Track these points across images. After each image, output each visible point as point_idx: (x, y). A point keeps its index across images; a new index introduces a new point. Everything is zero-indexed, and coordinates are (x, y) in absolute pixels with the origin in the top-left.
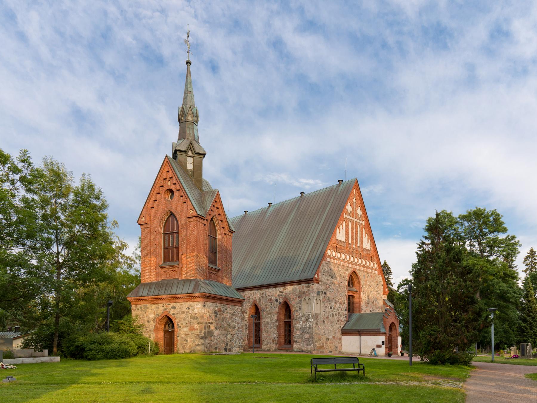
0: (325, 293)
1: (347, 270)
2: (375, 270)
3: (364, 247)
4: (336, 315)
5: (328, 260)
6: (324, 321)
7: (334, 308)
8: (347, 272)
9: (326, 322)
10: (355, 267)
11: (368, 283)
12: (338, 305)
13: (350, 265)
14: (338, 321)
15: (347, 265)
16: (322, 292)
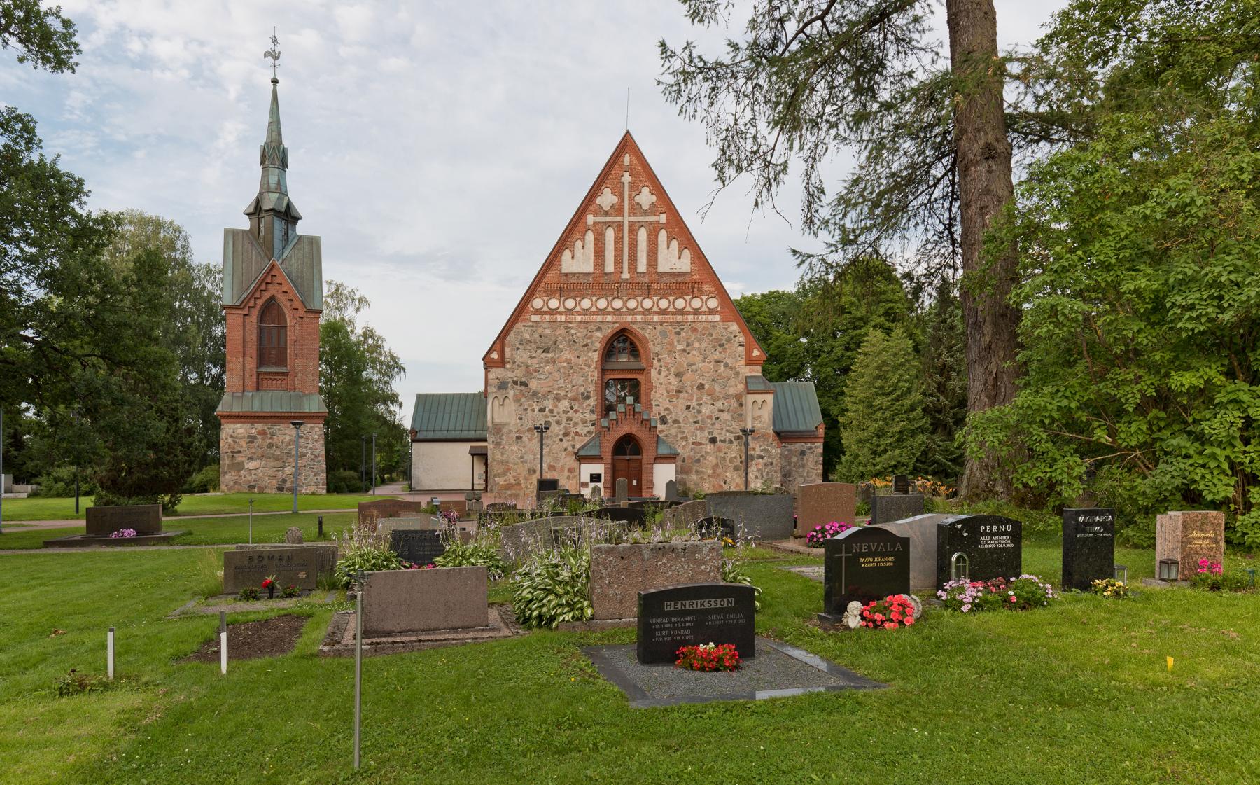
0: (524, 384)
1: (599, 329)
3: (661, 269)
4: (558, 423)
5: (535, 318)
6: (519, 438)
8: (598, 334)
9: (525, 439)
10: (630, 318)
11: (680, 347)
12: (564, 404)
13: (609, 318)
14: (566, 434)
15: (599, 318)
16: (516, 383)
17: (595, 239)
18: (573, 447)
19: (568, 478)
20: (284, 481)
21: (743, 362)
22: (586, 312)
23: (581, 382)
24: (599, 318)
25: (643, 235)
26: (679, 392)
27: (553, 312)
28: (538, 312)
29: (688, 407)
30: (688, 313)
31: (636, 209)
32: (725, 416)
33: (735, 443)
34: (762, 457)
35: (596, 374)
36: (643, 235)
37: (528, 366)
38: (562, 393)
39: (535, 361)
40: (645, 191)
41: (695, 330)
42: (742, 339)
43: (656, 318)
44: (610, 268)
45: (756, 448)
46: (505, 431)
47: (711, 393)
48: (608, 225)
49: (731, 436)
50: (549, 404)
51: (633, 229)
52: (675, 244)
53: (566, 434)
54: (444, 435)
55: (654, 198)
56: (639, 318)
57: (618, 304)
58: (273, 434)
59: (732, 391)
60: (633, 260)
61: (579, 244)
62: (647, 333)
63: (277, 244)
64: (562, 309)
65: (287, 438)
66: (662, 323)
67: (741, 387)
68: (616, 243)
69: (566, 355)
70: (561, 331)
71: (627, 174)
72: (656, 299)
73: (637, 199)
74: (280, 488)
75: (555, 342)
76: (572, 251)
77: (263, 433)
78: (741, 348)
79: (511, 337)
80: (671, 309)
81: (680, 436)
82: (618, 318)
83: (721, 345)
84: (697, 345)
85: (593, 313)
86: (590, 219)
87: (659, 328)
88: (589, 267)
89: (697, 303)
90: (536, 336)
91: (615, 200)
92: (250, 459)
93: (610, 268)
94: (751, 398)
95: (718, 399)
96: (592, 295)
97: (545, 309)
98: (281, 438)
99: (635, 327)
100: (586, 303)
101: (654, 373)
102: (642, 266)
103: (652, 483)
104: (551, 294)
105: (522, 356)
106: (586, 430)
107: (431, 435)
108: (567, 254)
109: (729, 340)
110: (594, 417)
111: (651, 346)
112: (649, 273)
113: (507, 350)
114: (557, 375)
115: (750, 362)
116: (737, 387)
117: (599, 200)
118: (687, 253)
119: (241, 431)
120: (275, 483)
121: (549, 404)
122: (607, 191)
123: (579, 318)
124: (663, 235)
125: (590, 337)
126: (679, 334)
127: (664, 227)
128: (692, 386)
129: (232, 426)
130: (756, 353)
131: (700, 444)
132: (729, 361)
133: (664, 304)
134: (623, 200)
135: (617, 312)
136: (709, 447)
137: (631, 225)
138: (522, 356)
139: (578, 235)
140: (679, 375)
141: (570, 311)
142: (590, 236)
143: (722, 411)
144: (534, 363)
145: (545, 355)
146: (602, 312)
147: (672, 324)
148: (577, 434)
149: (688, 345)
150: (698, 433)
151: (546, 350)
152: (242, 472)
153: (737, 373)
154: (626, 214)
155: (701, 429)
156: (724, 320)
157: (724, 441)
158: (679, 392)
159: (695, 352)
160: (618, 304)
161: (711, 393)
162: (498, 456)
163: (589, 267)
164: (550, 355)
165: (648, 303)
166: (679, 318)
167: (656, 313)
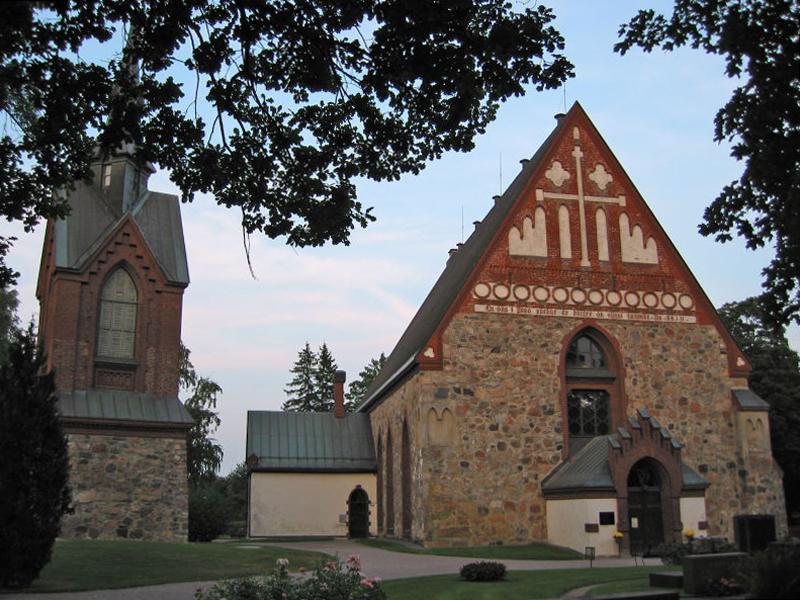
1: (559, 326)
2: (687, 312)
3: (626, 258)
6: (465, 465)
7: (506, 429)
8: (559, 332)
10: (594, 315)
11: (655, 352)
13: (571, 313)
15: (559, 313)
16: (458, 391)
18: (536, 477)
19: (531, 519)
20: (128, 521)
21: (726, 373)
22: (539, 304)
23: (541, 391)
25: (601, 218)
26: (659, 407)
27: (501, 302)
28: (482, 300)
30: (662, 312)
31: (590, 188)
32: (714, 438)
33: (728, 471)
34: (762, 490)
35: (559, 382)
36: (601, 218)
37: (473, 370)
38: (519, 406)
39: (481, 363)
40: (600, 169)
41: (670, 333)
42: (722, 345)
43: (625, 316)
44: (566, 252)
45: (756, 479)
46: (445, 454)
47: (695, 409)
48: (564, 203)
49: (723, 464)
50: (501, 418)
51: (591, 210)
52: (638, 230)
53: (526, 461)
54: (293, 464)
55: (610, 178)
56: (606, 315)
57: (579, 296)
58: (115, 451)
59: (719, 407)
61: (527, 222)
62: (616, 334)
63: (126, 198)
64: (512, 299)
65: (135, 458)
67: (728, 403)
70: (513, 325)
71: (577, 149)
74: (122, 532)
75: (507, 340)
76: (520, 229)
77: (102, 449)
78: (723, 356)
79: (449, 332)
80: (641, 306)
82: (582, 314)
83: (701, 352)
84: (674, 350)
87: (630, 328)
88: (541, 250)
89: (669, 301)
90: (482, 330)
91: (567, 175)
93: (566, 252)
94: (744, 416)
95: (703, 416)
97: (492, 297)
99: (600, 324)
100: (541, 294)
101: (628, 383)
102: (604, 254)
104: (500, 279)
105: (465, 356)
106: (550, 456)
107: (275, 464)
108: (514, 233)
109: (708, 346)
110: (560, 438)
111: (622, 350)
113: (446, 347)
114: (510, 382)
115: (735, 372)
116: (723, 404)
117: (548, 174)
118: (652, 242)
121: (501, 418)
122: (557, 165)
123: (534, 311)
124: (624, 221)
125: (549, 336)
126: (652, 335)
128: (674, 401)
130: (741, 362)
132: (712, 371)
134: (576, 176)
135: (578, 306)
137: (588, 205)
138: (465, 356)
139: (527, 212)
140: (656, 386)
141: (521, 303)
142: (540, 215)
143: (709, 432)
146: (562, 305)
147: (645, 324)
148: (539, 460)
149: (665, 349)
151: (496, 350)
153: (722, 386)
156: (701, 321)
157: (715, 470)
158: (659, 407)
161: (695, 409)
163: (541, 250)
164: (501, 356)
166: (652, 317)
167: (623, 309)
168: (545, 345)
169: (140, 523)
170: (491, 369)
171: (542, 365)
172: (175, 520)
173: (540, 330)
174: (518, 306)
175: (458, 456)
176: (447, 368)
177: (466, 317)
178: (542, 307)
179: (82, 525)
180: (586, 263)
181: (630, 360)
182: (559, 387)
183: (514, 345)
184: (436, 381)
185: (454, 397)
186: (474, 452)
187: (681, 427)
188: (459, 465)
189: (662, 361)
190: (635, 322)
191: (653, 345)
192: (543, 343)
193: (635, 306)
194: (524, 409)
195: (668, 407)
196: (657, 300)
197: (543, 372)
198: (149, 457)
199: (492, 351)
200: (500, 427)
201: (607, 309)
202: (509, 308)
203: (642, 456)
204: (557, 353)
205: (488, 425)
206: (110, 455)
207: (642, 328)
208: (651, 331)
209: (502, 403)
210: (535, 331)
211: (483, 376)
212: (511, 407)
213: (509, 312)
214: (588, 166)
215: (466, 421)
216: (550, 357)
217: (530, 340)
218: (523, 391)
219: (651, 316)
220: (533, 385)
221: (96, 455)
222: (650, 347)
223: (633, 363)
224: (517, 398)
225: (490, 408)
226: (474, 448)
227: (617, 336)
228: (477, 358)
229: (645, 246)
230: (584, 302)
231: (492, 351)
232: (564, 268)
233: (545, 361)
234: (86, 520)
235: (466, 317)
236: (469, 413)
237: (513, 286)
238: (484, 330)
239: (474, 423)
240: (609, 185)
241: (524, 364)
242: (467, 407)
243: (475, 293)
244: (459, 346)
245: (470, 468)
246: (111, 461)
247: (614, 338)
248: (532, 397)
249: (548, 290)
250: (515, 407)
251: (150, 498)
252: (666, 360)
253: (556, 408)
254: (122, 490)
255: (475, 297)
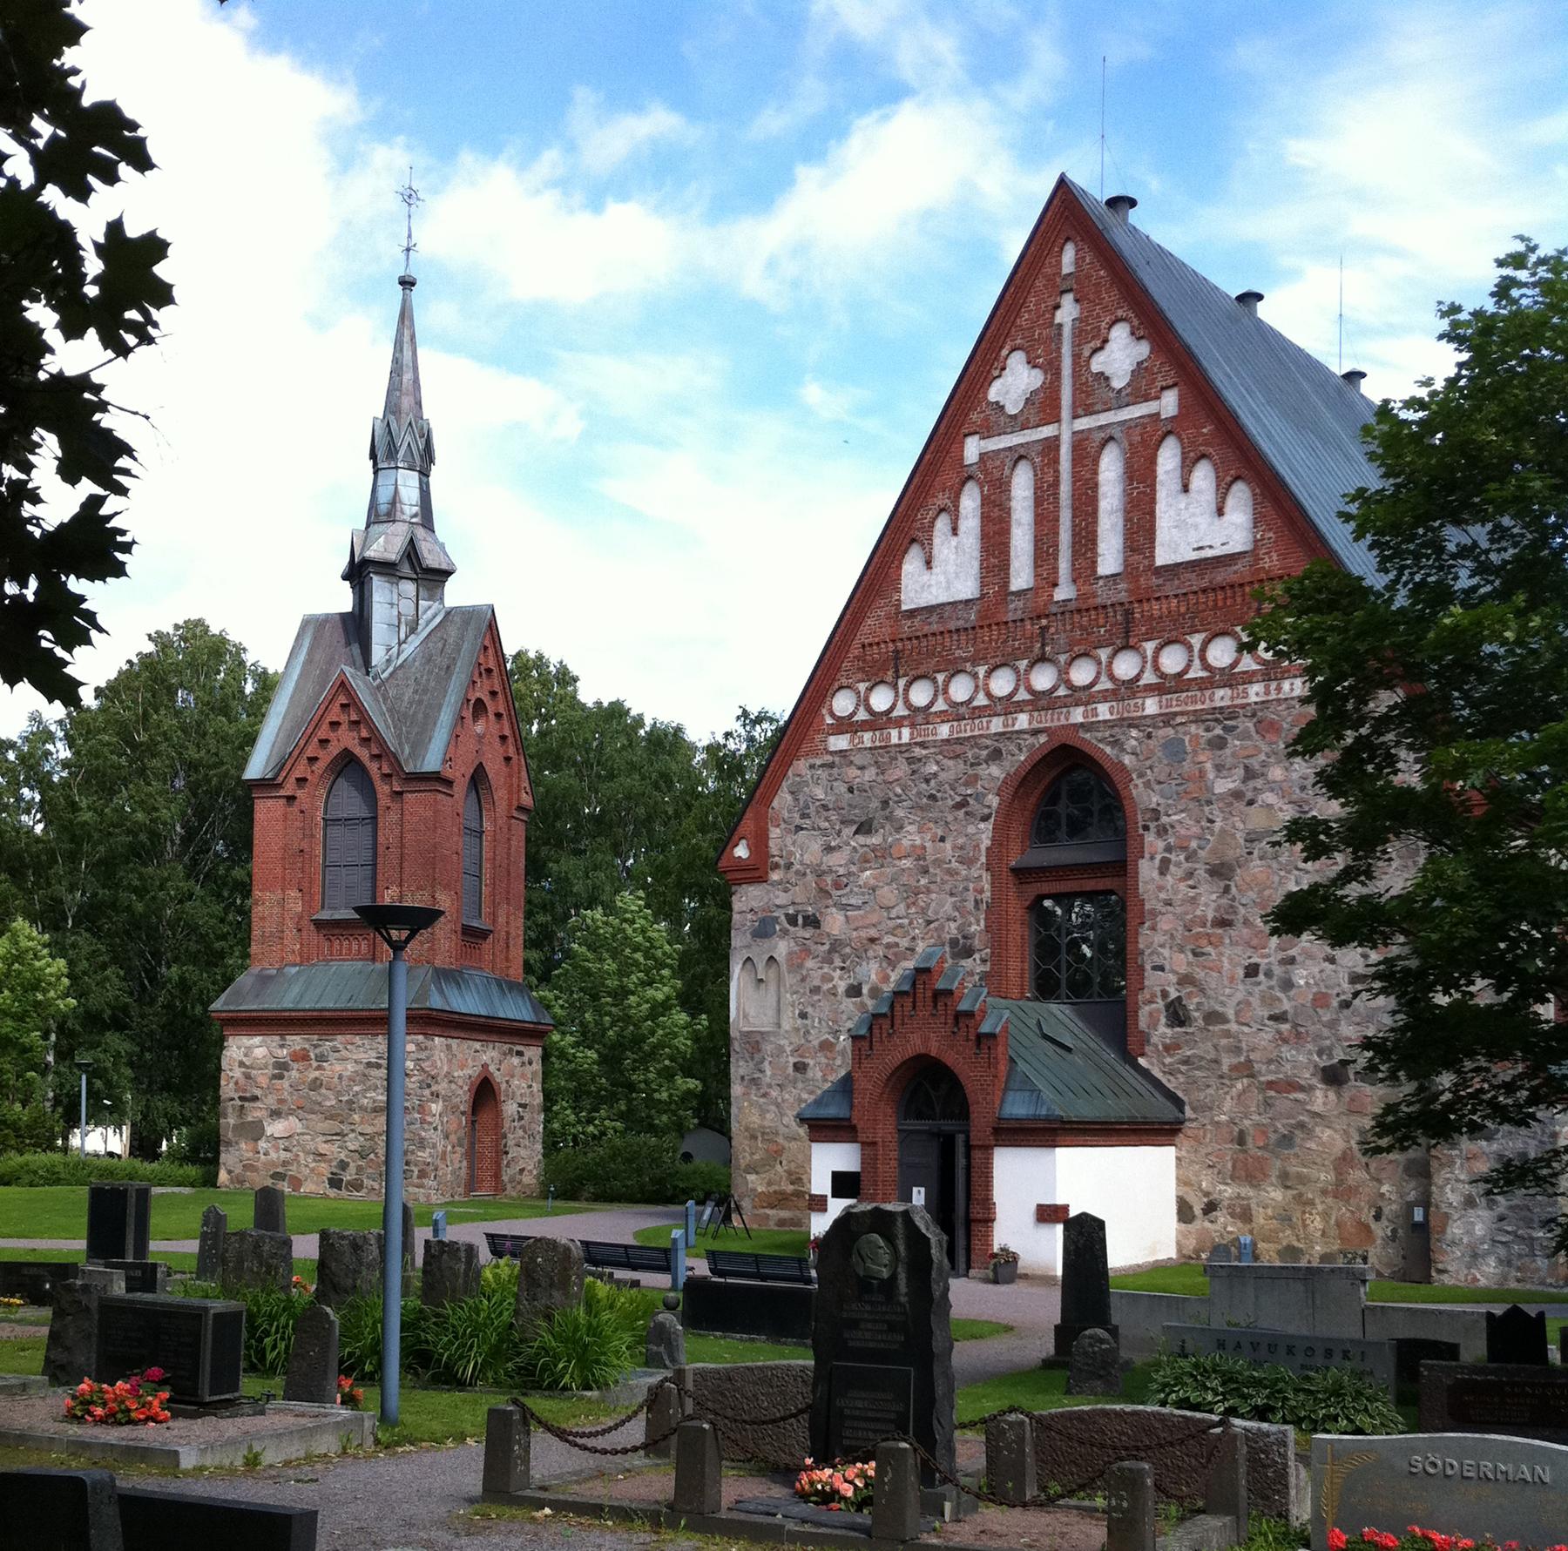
1: (996, 755)
5: (839, 742)
8: (995, 771)
10: (1077, 715)
11: (1222, 786)
13: (1022, 721)
15: (997, 725)
16: (792, 920)
17: (985, 502)
20: (343, 1165)
22: (957, 712)
24: (997, 725)
25: (1110, 468)
27: (880, 721)
28: (845, 725)
29: (1252, 971)
36: (1110, 468)
43: (1151, 706)
44: (1021, 576)
46: (768, 1048)
51: (1086, 453)
52: (1203, 476)
56: (1104, 711)
58: (321, 1058)
60: (1086, 541)
61: (942, 524)
62: (1127, 754)
65: (351, 1067)
66: (1167, 719)
68: (1038, 501)
69: (911, 837)
70: (901, 770)
71: (1068, 301)
72: (1149, 647)
73: (1097, 364)
75: (885, 803)
77: (302, 1057)
79: (783, 801)
80: (1196, 672)
81: (1227, 1061)
82: (1048, 720)
84: (1276, 773)
85: (978, 713)
86: (973, 449)
90: (841, 788)
92: (276, 1114)
93: (1021, 576)
96: (975, 661)
97: (862, 715)
98: (338, 1068)
99: (1087, 736)
100: (960, 689)
101: (1147, 870)
102: (1110, 559)
103: (988, 1204)
105: (807, 849)
112: (1130, 571)
113: (775, 832)
119: (260, 1052)
120: (325, 1169)
122: (1017, 361)
123: (944, 731)
125: (972, 780)
127: (1171, 428)
129: (246, 1041)
131: (1292, 1086)
133: (1172, 660)
135: (1041, 701)
136: (1322, 1099)
140: (1221, 871)
142: (970, 502)
144: (837, 860)
145: (861, 839)
146: (1007, 706)
147: (1198, 718)
149: (1250, 774)
150: (1287, 1052)
151: (864, 828)
152: (262, 1144)
154: (1065, 413)
155: (1298, 1036)
159: (1270, 798)
160: (1043, 679)
162: (754, 1119)
164: (875, 840)
165: (1126, 666)
166: (1222, 697)
167: (1150, 688)
168: (959, 806)
169: (359, 1168)
170: (854, 869)
171: (954, 848)
172: (407, 1164)
173: (954, 769)
174: (913, 726)
175: (788, 1049)
176: (775, 876)
177: (812, 767)
178: (960, 718)
179: (280, 1170)
180: (1064, 592)
181: (1155, 814)
182: (987, 895)
183: (900, 813)
184: (754, 904)
185: (785, 932)
186: (816, 1043)
187: (1278, 970)
188: (791, 1069)
189: (1239, 806)
190: (1176, 714)
191: (1219, 768)
192: (958, 799)
193: (1180, 675)
194: (912, 950)
195: (1246, 922)
196: (1203, 658)
197: (954, 865)
198: (369, 1065)
199: (856, 833)
200: (865, 990)
201: (1105, 696)
202: (894, 733)
203: (910, 1053)
204: (985, 819)
205: (842, 987)
206: (315, 1064)
207: (1193, 728)
208: (1218, 731)
209: (872, 940)
210: (943, 776)
211: (837, 886)
212: (889, 946)
213: (895, 740)
214: (1092, 336)
215: (803, 980)
216: (971, 829)
217: (932, 797)
218: (913, 910)
219: (1220, 693)
220: (934, 896)
221: (295, 1066)
222: (1211, 776)
223: (1164, 819)
224: (901, 926)
225: (848, 950)
226: (818, 1035)
227: (1127, 760)
228: (829, 849)
229: (1220, 512)
230: (1055, 688)
231: (856, 833)
232: (1010, 617)
233: (961, 841)
234: (285, 1163)
235: (812, 767)
236: (810, 964)
237: (902, 683)
238: (843, 789)
239: (817, 982)
240: (1140, 371)
241: (919, 854)
242: (807, 952)
243: (832, 714)
244: (799, 828)
245: (810, 1074)
246: (317, 1074)
247: (1123, 767)
248: (929, 923)
249: (975, 676)
250: (897, 945)
251: (369, 1130)
252: (1251, 803)
253: (976, 943)
254: (332, 1117)
255: (829, 720)
